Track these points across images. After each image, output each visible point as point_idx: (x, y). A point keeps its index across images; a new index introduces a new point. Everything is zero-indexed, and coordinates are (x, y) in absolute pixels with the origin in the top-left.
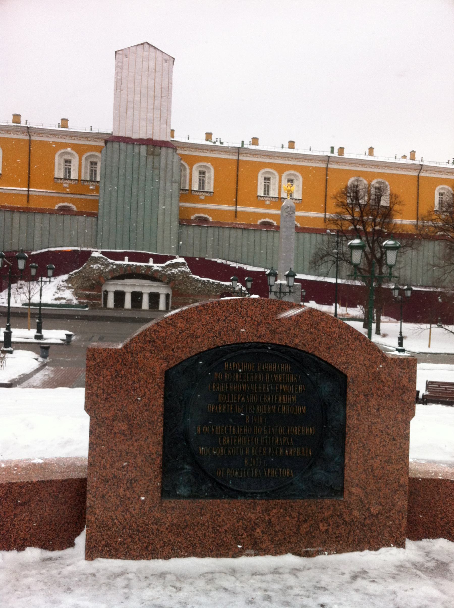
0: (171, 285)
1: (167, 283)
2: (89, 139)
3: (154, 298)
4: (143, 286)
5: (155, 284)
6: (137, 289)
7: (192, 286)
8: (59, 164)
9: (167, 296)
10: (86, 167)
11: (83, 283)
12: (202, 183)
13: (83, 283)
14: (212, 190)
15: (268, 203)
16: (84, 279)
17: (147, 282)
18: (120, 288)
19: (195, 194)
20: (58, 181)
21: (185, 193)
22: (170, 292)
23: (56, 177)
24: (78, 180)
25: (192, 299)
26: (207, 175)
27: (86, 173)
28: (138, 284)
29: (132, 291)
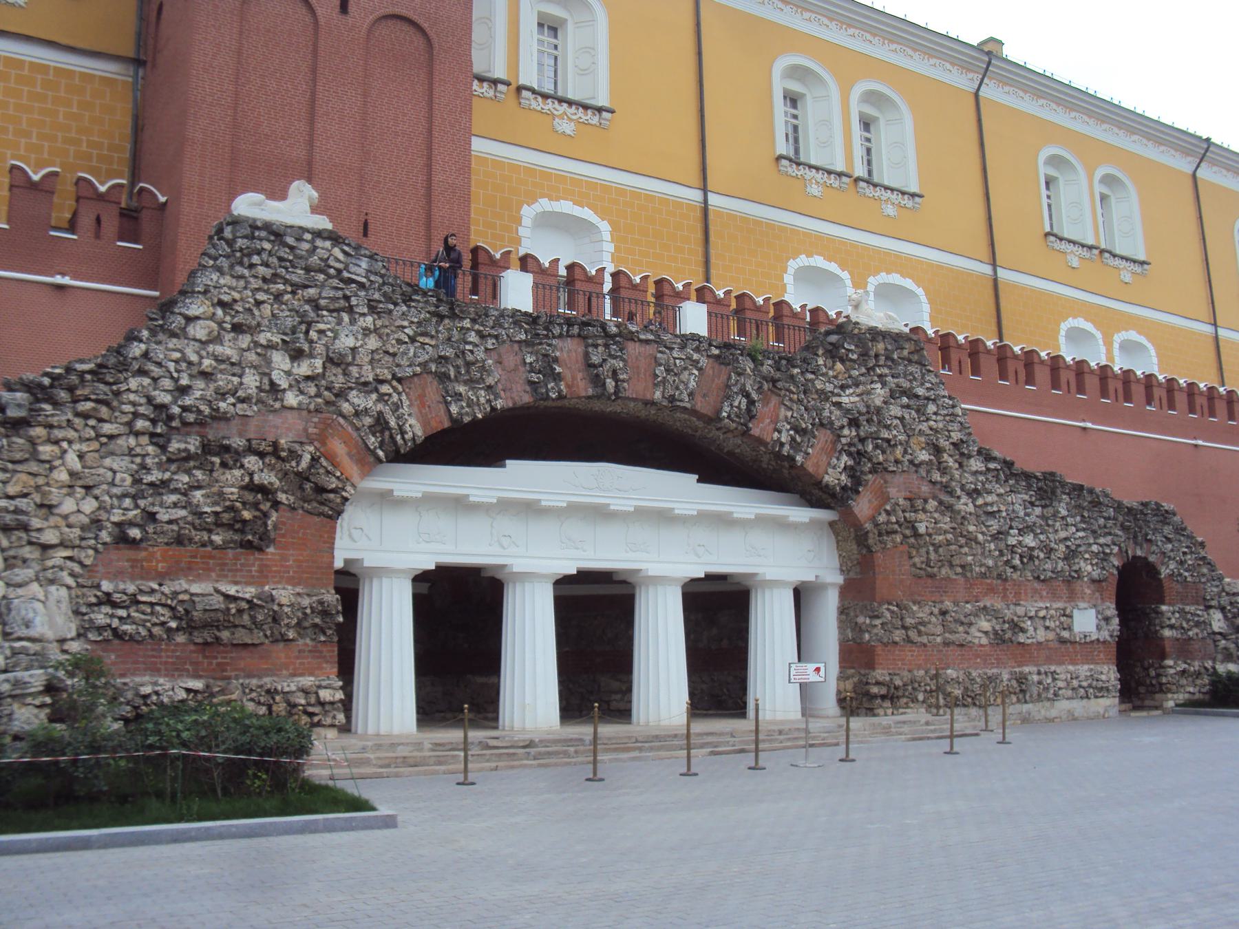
3: (718, 612)
4: (663, 518)
11: (160, 487)
13: (160, 487)
14: (602, 102)
16: (160, 442)
17: (677, 490)
18: (466, 546)
19: (534, 105)
21: (491, 93)
26: (572, 37)
28: (627, 505)
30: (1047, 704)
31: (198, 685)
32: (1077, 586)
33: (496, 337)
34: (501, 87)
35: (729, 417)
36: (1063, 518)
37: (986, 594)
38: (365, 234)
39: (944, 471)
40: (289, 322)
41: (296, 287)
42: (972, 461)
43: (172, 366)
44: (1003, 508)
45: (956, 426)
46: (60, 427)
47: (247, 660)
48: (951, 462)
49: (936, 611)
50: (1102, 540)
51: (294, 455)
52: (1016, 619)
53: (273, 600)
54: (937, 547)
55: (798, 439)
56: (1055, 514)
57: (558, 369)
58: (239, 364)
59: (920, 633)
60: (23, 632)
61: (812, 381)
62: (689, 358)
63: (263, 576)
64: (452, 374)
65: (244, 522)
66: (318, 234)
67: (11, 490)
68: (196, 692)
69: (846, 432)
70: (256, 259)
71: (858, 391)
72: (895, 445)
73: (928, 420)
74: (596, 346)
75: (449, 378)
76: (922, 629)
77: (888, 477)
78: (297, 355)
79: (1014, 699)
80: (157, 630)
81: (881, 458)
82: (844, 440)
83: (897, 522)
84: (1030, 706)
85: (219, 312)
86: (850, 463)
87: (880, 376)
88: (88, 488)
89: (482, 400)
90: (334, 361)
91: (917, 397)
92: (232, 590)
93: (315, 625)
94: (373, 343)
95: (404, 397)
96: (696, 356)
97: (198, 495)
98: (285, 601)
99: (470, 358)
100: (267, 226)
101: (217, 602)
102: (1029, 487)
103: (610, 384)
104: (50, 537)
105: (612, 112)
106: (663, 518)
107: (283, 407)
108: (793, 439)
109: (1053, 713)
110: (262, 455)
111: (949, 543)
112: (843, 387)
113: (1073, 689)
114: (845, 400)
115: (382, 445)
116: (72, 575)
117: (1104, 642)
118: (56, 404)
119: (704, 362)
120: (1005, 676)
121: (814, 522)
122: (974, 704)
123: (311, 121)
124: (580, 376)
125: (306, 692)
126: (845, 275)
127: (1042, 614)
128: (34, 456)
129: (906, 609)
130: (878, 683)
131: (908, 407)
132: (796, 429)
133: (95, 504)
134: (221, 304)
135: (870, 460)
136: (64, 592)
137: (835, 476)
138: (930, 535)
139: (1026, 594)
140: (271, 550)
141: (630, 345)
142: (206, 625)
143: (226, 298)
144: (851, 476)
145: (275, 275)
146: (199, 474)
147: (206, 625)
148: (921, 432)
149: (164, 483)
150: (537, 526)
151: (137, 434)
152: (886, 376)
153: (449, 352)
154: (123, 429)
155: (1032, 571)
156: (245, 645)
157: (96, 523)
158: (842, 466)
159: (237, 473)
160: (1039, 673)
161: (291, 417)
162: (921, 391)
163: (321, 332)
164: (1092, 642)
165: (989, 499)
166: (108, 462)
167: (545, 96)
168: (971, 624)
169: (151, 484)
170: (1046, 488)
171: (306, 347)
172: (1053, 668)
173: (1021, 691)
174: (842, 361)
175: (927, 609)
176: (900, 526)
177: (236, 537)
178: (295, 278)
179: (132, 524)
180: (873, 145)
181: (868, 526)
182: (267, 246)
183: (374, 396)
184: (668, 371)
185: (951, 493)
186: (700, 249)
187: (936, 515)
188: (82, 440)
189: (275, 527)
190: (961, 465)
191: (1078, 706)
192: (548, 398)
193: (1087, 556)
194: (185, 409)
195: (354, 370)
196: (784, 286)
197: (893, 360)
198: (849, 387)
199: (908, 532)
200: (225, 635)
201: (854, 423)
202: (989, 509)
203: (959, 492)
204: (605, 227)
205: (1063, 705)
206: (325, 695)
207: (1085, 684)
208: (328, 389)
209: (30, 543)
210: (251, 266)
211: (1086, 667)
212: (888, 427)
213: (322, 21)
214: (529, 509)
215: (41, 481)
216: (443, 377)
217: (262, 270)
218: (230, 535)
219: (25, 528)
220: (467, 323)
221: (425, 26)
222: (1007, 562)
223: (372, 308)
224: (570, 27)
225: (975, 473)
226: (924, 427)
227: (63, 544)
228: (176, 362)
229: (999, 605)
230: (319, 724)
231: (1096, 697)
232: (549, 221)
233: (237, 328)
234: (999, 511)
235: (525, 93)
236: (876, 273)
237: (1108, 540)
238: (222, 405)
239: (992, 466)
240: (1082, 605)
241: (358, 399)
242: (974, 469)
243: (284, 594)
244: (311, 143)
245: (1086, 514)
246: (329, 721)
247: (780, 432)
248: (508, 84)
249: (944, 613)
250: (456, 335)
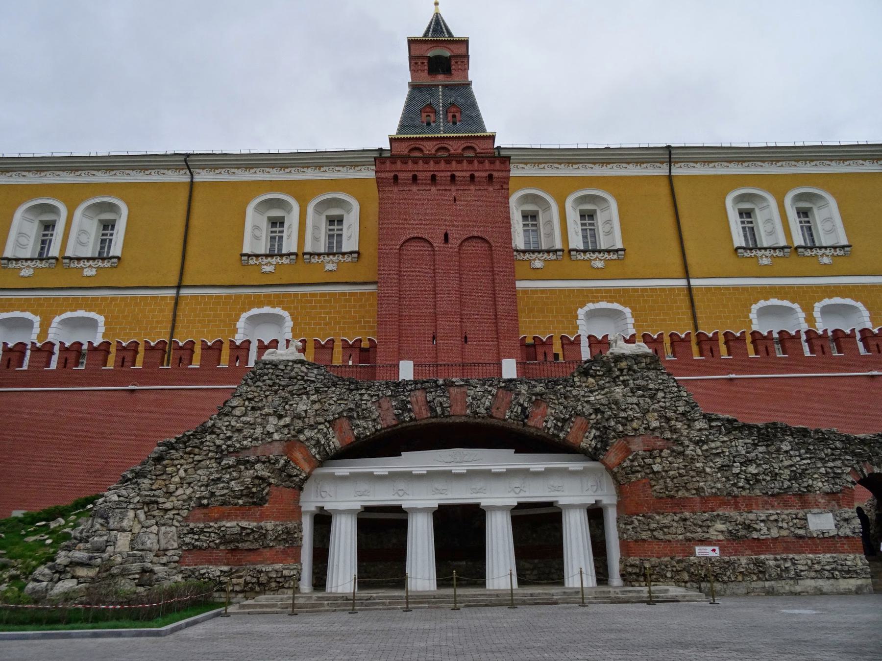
0: (612, 458)
1: (592, 455)
2: (323, 169)
5: (537, 463)
6: (459, 495)
7: (708, 456)
8: (256, 227)
9: (595, 514)
10: (316, 228)
12: (589, 234)
14: (619, 245)
15: (765, 261)
16: (219, 461)
17: (500, 460)
19: (579, 257)
20: (251, 262)
21: (555, 257)
22: (608, 497)
23: (246, 250)
25: (726, 519)
26: (600, 218)
27: (316, 239)
29: (435, 504)
30: (792, 582)
31: (225, 568)
32: (811, 497)
33: (378, 395)
34: (559, 253)
35: (510, 418)
36: (786, 452)
37: (720, 506)
38: (466, 342)
39: (674, 430)
40: (277, 403)
41: (284, 387)
42: (696, 423)
43: (224, 428)
44: (725, 450)
45: (681, 403)
46: (177, 459)
47: (251, 557)
48: (679, 425)
49: (676, 518)
50: (831, 464)
51: (277, 461)
52: (747, 522)
53: (262, 528)
54: (673, 478)
55: (559, 424)
56: (778, 450)
57: (409, 406)
58: (254, 424)
59: (665, 534)
60: (141, 547)
61: (570, 391)
62: (486, 391)
63: (262, 518)
64: (355, 416)
65: (253, 493)
66: (294, 362)
67: (154, 487)
68: (225, 572)
69: (593, 416)
70: (266, 378)
71: (603, 392)
72: (632, 420)
73: (659, 402)
74: (431, 392)
75: (354, 418)
76: (666, 530)
77: (629, 439)
78: (280, 417)
79: (755, 578)
80: (212, 544)
81: (621, 428)
82: (592, 422)
83: (639, 465)
84: (773, 582)
85: (247, 403)
86: (598, 434)
87: (623, 381)
88: (189, 484)
89: (370, 426)
90: (299, 417)
91: (650, 389)
92: (244, 524)
93: (284, 539)
94: (317, 406)
95: (331, 429)
96: (489, 389)
97: (233, 483)
98: (269, 528)
99: (364, 407)
100: (271, 363)
101: (237, 530)
102: (751, 434)
103: (439, 410)
104: (168, 505)
105: (624, 250)
106: (487, 474)
107: (273, 441)
108: (556, 425)
109: (798, 589)
110: (264, 463)
111: (681, 475)
112: (591, 392)
113: (816, 571)
114: (592, 398)
115: (319, 453)
116: (177, 521)
117: (847, 537)
118: (177, 450)
119: (494, 391)
120: (744, 561)
121: (584, 468)
122: (718, 581)
123: (435, 294)
124: (423, 408)
125: (277, 571)
126: (796, 306)
127: (772, 518)
128: (165, 473)
129: (649, 518)
130: (632, 566)
131: (643, 396)
132: (557, 419)
133: (191, 490)
134: (250, 400)
135: (614, 430)
136: (174, 528)
137: (588, 441)
138: (667, 471)
139: (757, 505)
140: (267, 505)
141: (452, 390)
142: (231, 541)
143: (250, 396)
144: (602, 442)
145: (274, 383)
146: (235, 474)
147: (231, 541)
148: (654, 410)
149: (219, 479)
150: (420, 485)
151: (210, 459)
152: (628, 380)
153: (352, 406)
154: (205, 457)
155: (761, 490)
156: (250, 550)
157: (190, 498)
158: (592, 435)
159: (251, 472)
160: (776, 559)
161: (276, 444)
162: (651, 386)
163: (291, 405)
164: (833, 537)
165: (713, 445)
166: (199, 472)
167: (585, 252)
168: (709, 527)
169: (213, 480)
170: (768, 434)
171: (283, 413)
172: (791, 556)
173: (760, 572)
174: (593, 377)
175: (669, 518)
176: (643, 467)
177: (251, 500)
178: (282, 383)
179: (204, 498)
180: (812, 224)
181: (615, 470)
182: (271, 371)
183: (316, 431)
184: (473, 399)
185: (682, 444)
186: (689, 311)
187: (670, 459)
188: (187, 464)
189: (267, 494)
190: (689, 426)
191: (824, 584)
192: (405, 421)
193: (816, 476)
194: (228, 446)
195: (306, 420)
196: (751, 321)
197: (634, 371)
198: (595, 391)
199: (648, 471)
200: (240, 545)
201: (597, 411)
202: (714, 451)
203: (687, 443)
204: (627, 311)
205: (808, 584)
206: (286, 573)
207: (828, 567)
208: (294, 430)
209: (158, 509)
210: (264, 381)
211: (828, 555)
212: (624, 410)
213: (436, 249)
214: (408, 476)
215: (167, 482)
216: (350, 418)
217: (268, 382)
218: (245, 499)
219: (157, 503)
220: (363, 391)
221: (487, 238)
222: (734, 485)
223: (317, 391)
224: (598, 212)
225: (700, 430)
226: (656, 406)
227: (173, 508)
228: (227, 426)
229: (734, 514)
230: (283, 587)
231: (845, 578)
232: (592, 315)
233: (253, 409)
234: (723, 452)
235: (572, 253)
236: (820, 299)
237: (838, 463)
238: (245, 443)
239: (714, 424)
240: (816, 510)
241: (308, 433)
242: (698, 427)
243: (269, 525)
244: (435, 305)
245: (811, 447)
246: (287, 585)
247: (547, 422)
248: (563, 250)
249: (685, 520)
250: (358, 397)
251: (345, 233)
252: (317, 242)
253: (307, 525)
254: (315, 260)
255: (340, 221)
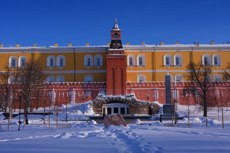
9: (128, 108)
24: (93, 66)
251: (100, 61)
252: (96, 64)
253: (103, 109)
254: (96, 67)
255: (99, 59)
